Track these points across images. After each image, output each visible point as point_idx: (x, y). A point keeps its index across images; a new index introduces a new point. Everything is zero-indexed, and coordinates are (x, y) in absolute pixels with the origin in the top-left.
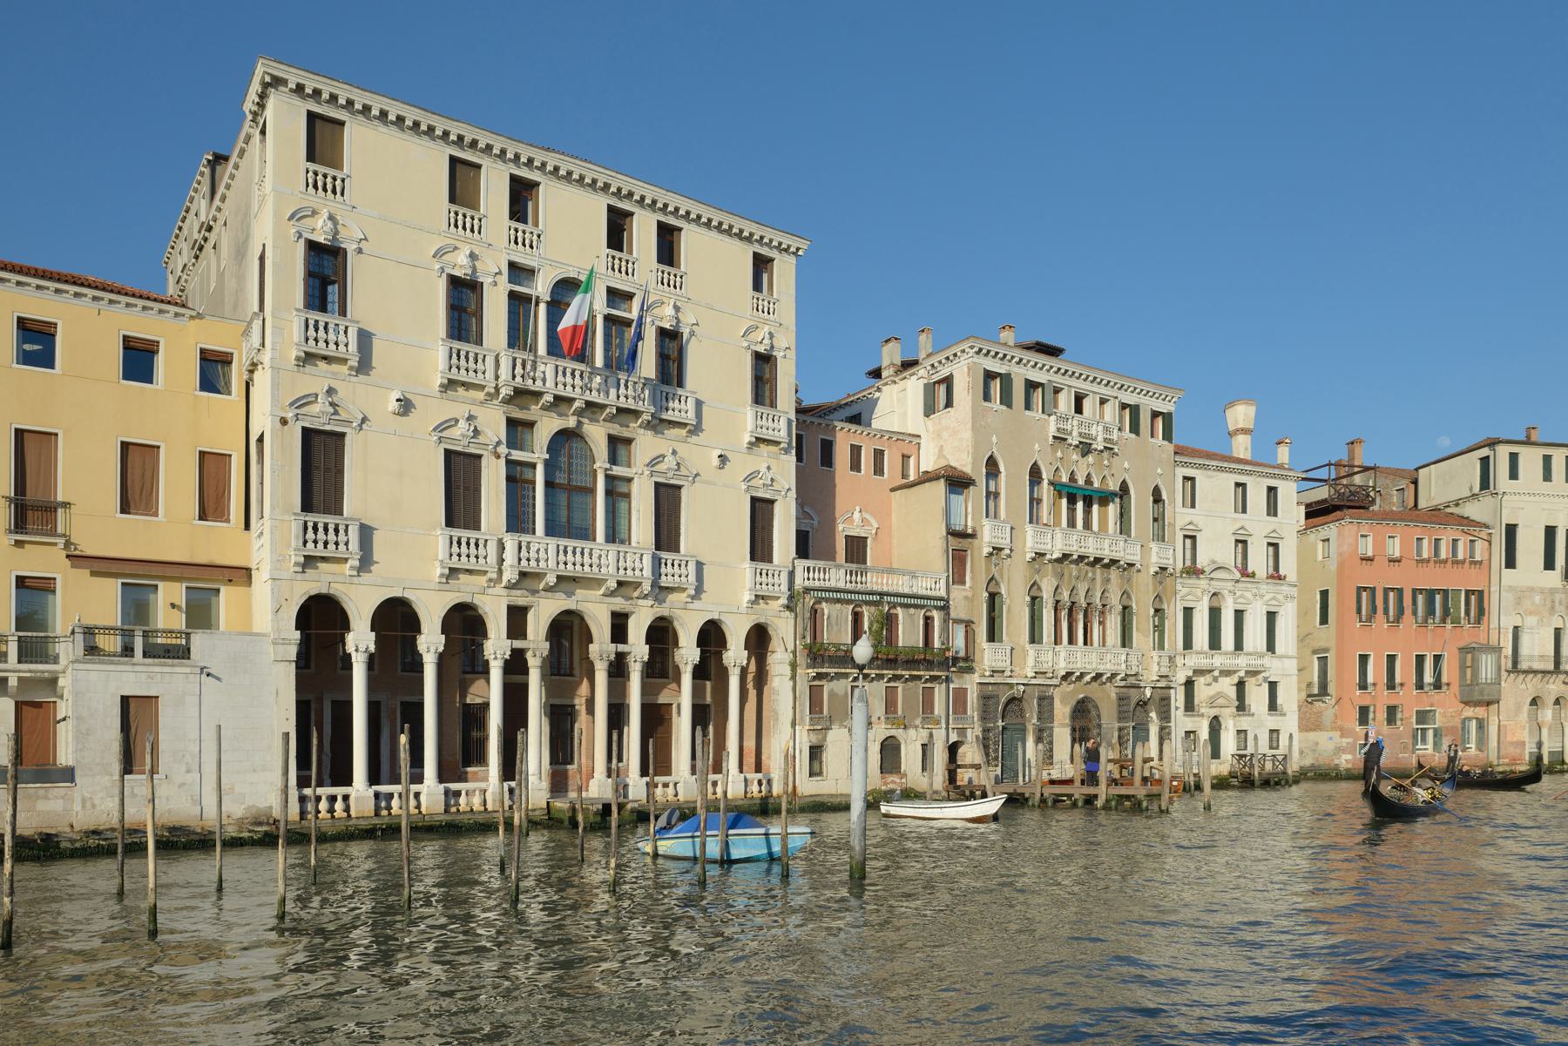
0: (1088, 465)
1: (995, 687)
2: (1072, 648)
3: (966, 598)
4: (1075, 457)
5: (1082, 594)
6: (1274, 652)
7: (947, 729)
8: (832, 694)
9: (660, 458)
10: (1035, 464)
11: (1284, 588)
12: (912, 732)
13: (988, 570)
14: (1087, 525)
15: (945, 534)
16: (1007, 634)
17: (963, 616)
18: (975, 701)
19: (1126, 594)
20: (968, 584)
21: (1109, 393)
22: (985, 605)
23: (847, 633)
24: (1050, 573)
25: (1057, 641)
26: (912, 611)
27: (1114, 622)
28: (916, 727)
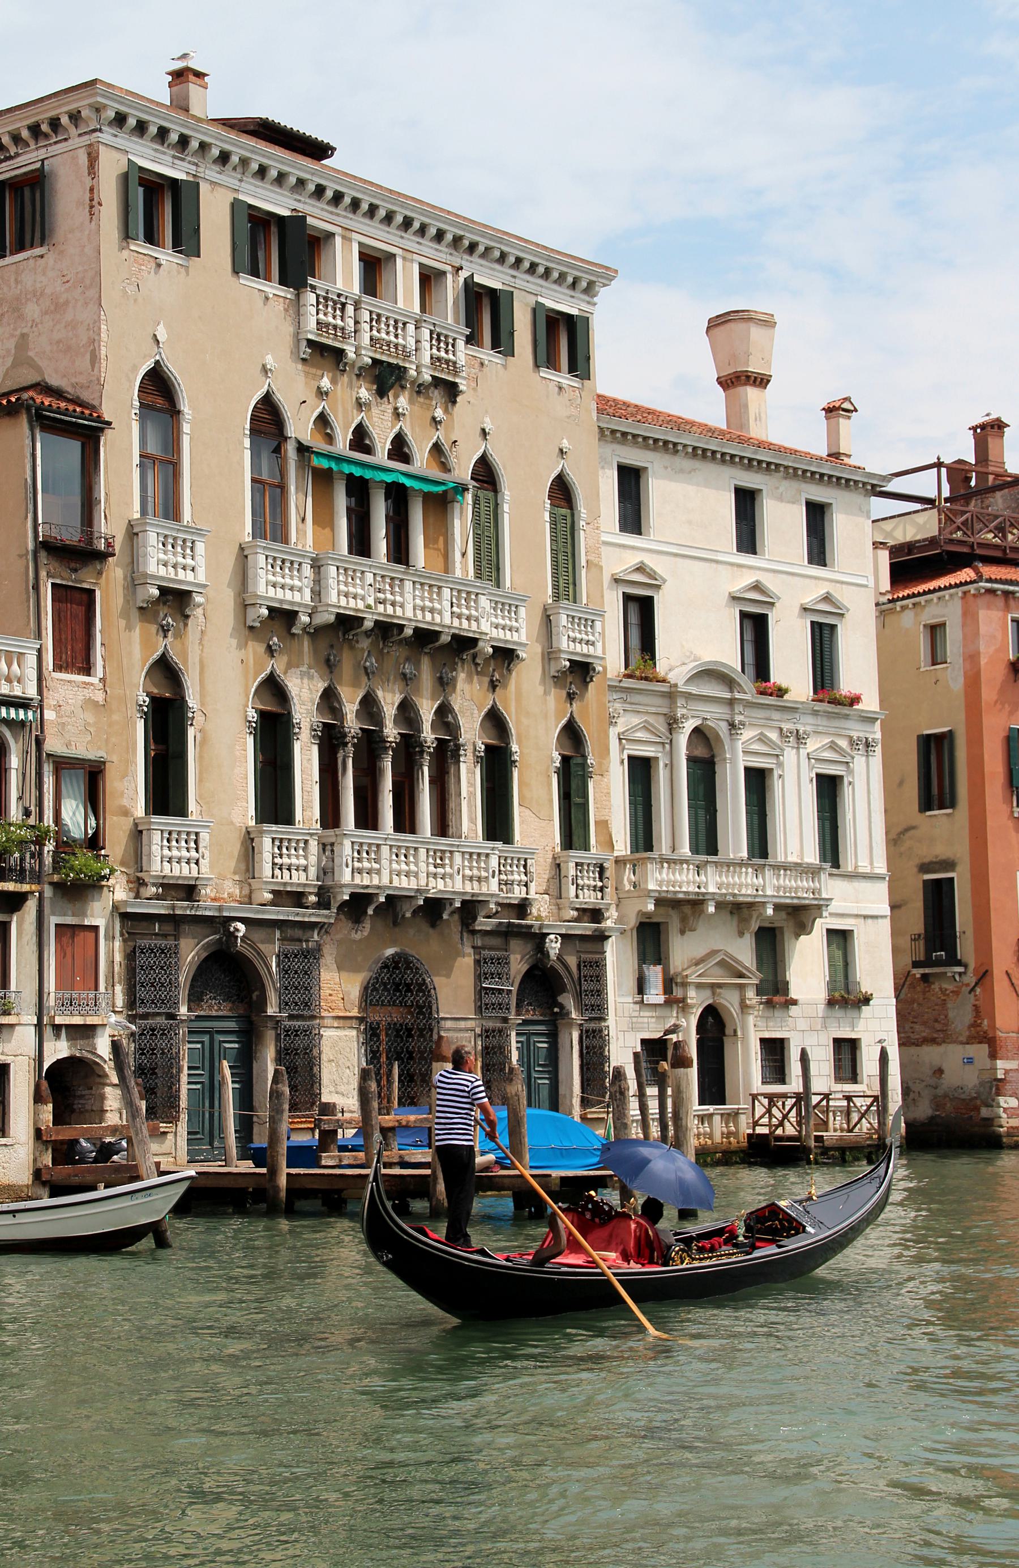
6: (836, 864)
7: (39, 1026)
11: (849, 724)
13: (147, 644)
14: (400, 553)
15: (31, 546)
17: (83, 749)
19: (495, 720)
20: (100, 673)
21: (443, 257)
22: (140, 725)
25: (330, 817)
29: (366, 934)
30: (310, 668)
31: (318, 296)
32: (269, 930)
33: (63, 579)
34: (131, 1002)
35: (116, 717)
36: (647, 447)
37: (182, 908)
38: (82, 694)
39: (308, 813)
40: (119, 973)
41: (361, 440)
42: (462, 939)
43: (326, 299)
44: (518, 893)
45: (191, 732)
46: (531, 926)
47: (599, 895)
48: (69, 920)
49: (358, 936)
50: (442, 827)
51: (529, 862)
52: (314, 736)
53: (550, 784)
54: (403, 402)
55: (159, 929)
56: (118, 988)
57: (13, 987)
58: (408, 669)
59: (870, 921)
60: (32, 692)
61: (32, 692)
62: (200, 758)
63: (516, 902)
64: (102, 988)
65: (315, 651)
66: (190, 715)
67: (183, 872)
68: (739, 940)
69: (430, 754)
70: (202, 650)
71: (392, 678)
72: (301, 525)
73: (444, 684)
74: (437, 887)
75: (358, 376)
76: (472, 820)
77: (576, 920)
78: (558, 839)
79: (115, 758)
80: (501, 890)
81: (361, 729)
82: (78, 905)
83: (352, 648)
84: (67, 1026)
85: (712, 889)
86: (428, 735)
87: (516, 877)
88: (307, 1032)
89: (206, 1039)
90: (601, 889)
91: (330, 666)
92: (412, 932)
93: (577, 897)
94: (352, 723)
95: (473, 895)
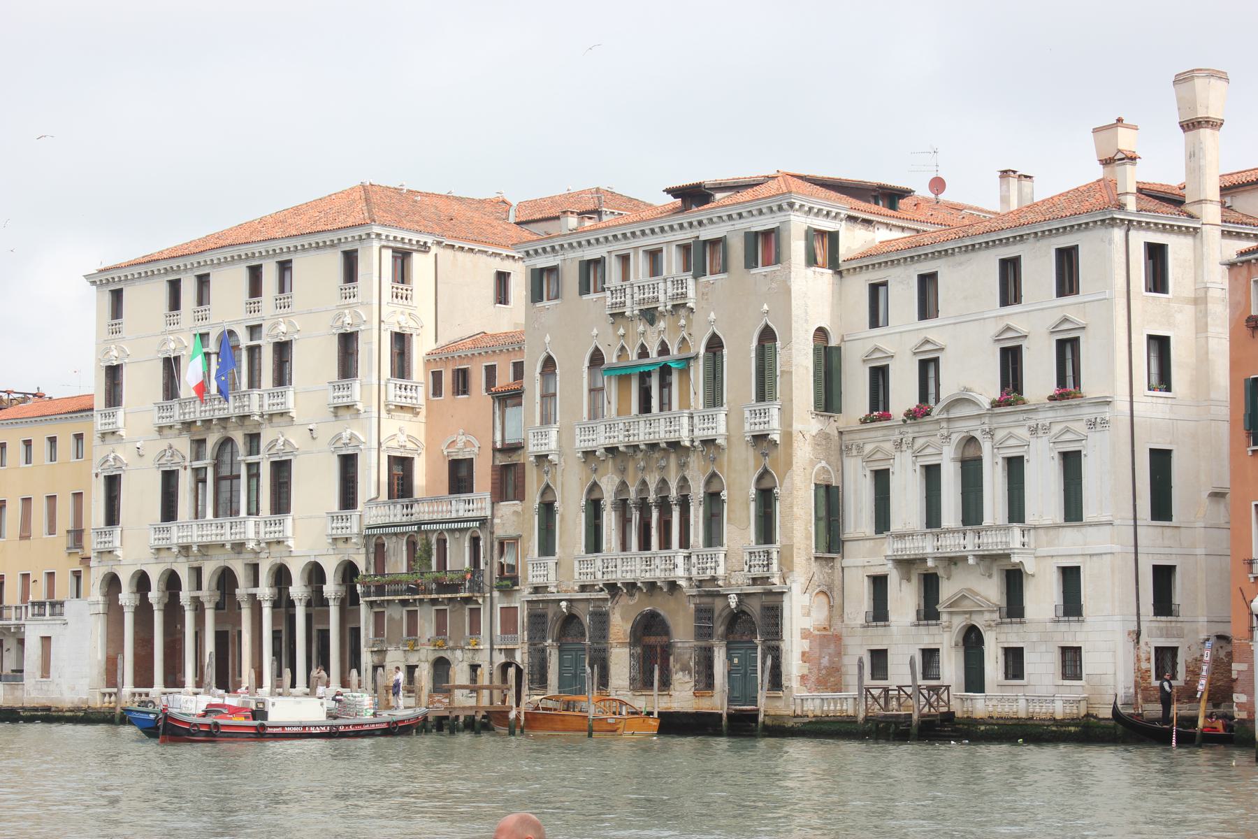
1: (545, 605)
2: (647, 554)
3: (516, 512)
4: (641, 328)
5: (652, 487)
7: (492, 649)
8: (391, 619)
9: (273, 443)
10: (597, 350)
12: (458, 653)
13: (539, 481)
16: (560, 545)
18: (525, 620)
21: (689, 236)
22: (536, 517)
23: (402, 563)
26: (457, 535)
27: (697, 515)
28: (462, 649)
31: (612, 291)
34: (530, 638)
35: (526, 516)
36: (933, 258)
37: (540, 597)
38: (512, 510)
41: (644, 353)
43: (616, 290)
44: (709, 573)
45: (557, 516)
46: (718, 591)
48: (505, 605)
50: (685, 543)
53: (748, 508)
54: (662, 324)
56: (526, 633)
58: (663, 463)
59: (1095, 558)
61: (488, 513)
62: (561, 528)
64: (519, 633)
65: (615, 465)
68: (989, 580)
69: (676, 504)
73: (683, 466)
74: (648, 576)
78: (753, 537)
79: (525, 535)
80: (698, 573)
81: (641, 498)
83: (633, 459)
85: (929, 550)
86: (674, 493)
87: (708, 565)
88: (604, 650)
89: (574, 653)
90: (768, 565)
91: (623, 471)
93: (749, 571)
94: (632, 495)
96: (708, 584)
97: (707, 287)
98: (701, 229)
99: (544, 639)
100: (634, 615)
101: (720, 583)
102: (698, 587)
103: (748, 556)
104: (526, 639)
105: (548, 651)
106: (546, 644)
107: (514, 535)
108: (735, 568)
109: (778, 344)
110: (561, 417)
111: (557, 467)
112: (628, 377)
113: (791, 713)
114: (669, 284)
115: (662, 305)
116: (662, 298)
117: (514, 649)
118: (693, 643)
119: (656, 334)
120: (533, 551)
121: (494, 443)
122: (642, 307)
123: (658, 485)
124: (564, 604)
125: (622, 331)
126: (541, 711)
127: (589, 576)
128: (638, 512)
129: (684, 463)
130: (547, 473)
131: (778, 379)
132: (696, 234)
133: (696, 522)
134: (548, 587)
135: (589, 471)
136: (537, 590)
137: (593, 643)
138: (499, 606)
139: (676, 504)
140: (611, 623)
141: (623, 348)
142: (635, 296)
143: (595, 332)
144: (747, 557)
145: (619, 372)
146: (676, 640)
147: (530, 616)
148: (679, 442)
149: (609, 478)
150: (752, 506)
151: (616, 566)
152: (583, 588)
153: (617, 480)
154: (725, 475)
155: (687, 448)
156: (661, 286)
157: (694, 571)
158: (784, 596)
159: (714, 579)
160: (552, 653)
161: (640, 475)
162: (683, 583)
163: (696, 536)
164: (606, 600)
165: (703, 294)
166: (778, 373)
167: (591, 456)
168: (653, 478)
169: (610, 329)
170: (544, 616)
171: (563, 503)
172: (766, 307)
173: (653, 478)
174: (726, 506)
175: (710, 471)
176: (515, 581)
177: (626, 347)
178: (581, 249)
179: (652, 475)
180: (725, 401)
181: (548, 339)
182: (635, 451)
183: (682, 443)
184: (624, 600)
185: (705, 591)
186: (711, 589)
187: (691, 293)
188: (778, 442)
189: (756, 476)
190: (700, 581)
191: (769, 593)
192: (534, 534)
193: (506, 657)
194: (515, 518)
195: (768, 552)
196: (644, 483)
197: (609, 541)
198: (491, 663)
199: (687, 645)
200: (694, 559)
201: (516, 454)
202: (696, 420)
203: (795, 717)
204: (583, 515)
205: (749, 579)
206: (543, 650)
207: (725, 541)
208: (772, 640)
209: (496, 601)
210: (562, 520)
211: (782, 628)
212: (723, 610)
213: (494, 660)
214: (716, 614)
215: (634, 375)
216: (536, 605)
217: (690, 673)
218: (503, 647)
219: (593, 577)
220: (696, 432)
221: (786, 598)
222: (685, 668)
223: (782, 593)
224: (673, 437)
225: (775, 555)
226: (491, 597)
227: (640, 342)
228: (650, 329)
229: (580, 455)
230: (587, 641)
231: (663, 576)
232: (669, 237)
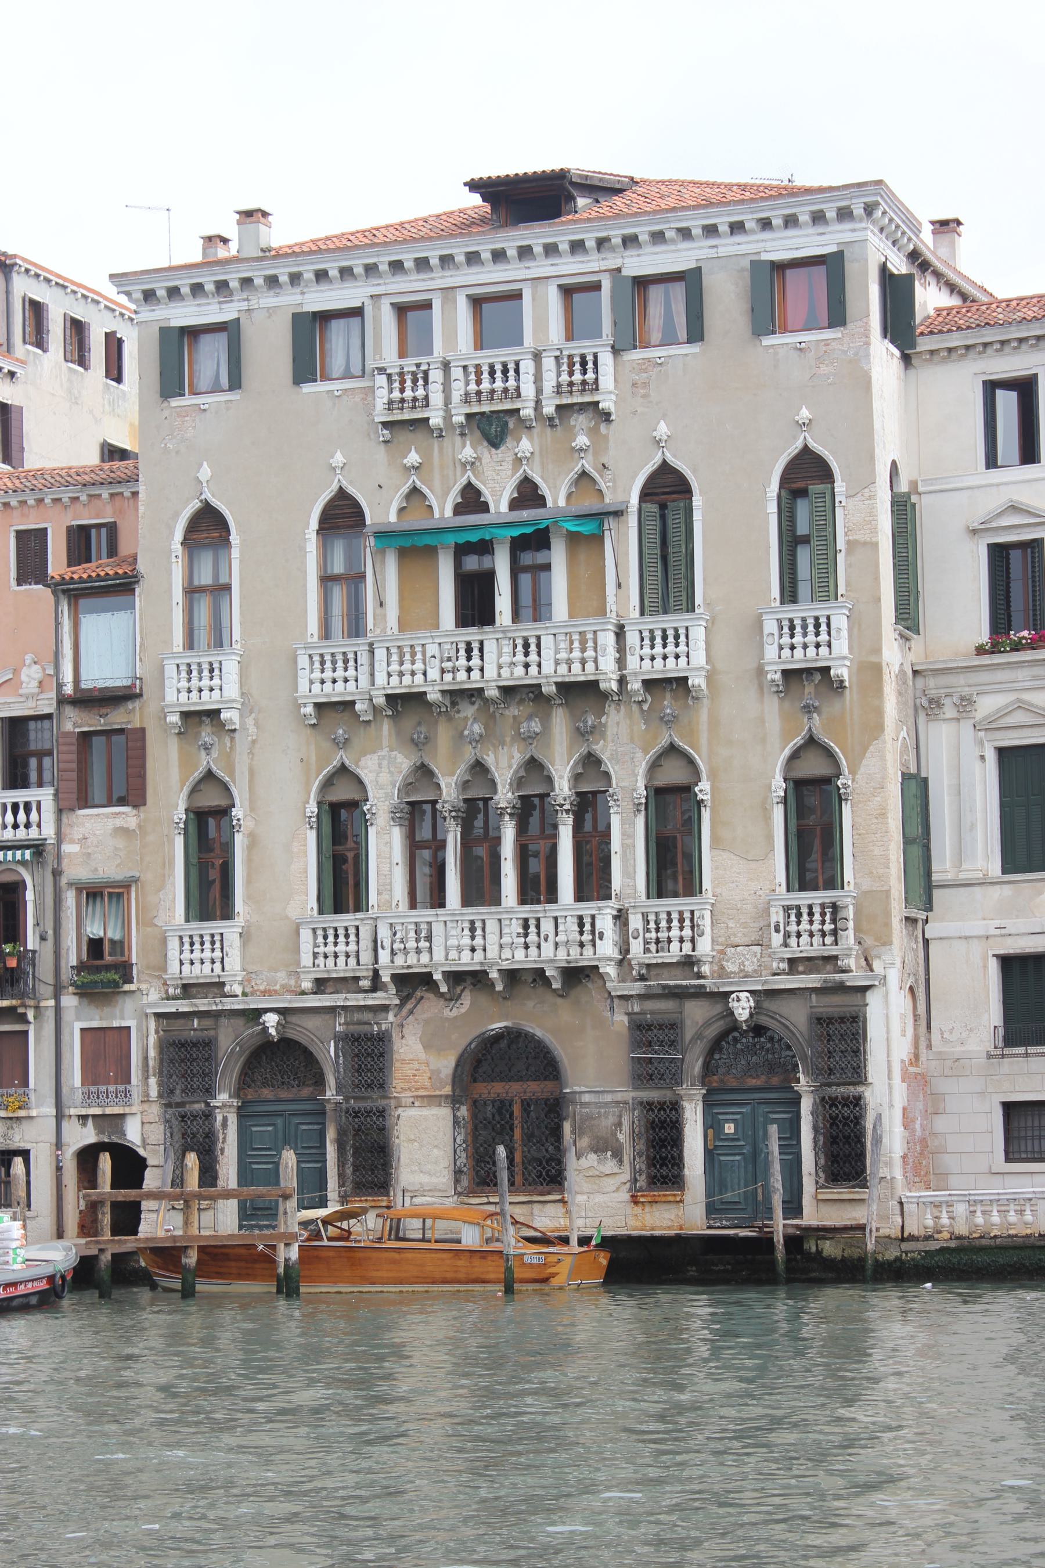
0: (518, 461)
1: (208, 1022)
3: (123, 832)
4: (468, 452)
7: (59, 1117)
13: (186, 763)
16: (248, 898)
18: (152, 1053)
21: (594, 266)
22: (179, 842)
24: (385, 742)
29: (463, 1010)
30: (391, 750)
31: (389, 376)
32: (327, 1017)
33: (90, 726)
34: (167, 1091)
37: (203, 1004)
38: (111, 824)
39: (386, 896)
40: (154, 1067)
42: (612, 1009)
44: (675, 952)
46: (703, 986)
47: (829, 940)
48: (95, 1024)
49: (447, 1013)
51: (697, 914)
52: (393, 819)
53: (768, 818)
54: (525, 445)
55: (199, 1024)
56: (153, 1081)
57: (32, 1085)
58: (536, 726)
60: (49, 831)
61: (49, 831)
62: (249, 861)
63: (674, 960)
64: (134, 1080)
65: (399, 733)
66: (235, 822)
67: (201, 972)
69: (567, 811)
70: (252, 759)
71: (508, 739)
72: (379, 610)
75: (462, 435)
76: (629, 874)
77: (782, 973)
79: (148, 877)
80: (647, 950)
81: (466, 801)
82: (106, 1010)
83: (450, 719)
84: (94, 1116)
88: (382, 1113)
90: (835, 932)
92: (530, 1004)
93: (786, 945)
95: (569, 962)
96: (665, 972)
97: (645, 371)
98: (628, 253)
99: (209, 1092)
100: (462, 1039)
101: (706, 969)
102: (642, 978)
103: (781, 913)
104: (154, 1092)
105: (219, 1118)
106: (214, 1103)
107: (119, 877)
108: (737, 940)
109: (840, 486)
110: (243, 632)
111: (237, 735)
112: (431, 551)
113: (895, 1232)
114: (548, 363)
115: (532, 404)
116: (528, 390)
117: (122, 1116)
118: (629, 1095)
119: (508, 466)
120: (172, 909)
121: (60, 686)
122: (476, 409)
123: (516, 772)
124: (271, 1020)
125: (413, 458)
126: (326, 1243)
127: (341, 960)
128: (459, 829)
129: (593, 727)
130: (207, 748)
131: (841, 558)
132: (613, 263)
133: (628, 848)
134: (223, 984)
135: (327, 745)
136: (188, 990)
137: (347, 1099)
138: (78, 1026)
139: (567, 811)
140: (396, 1056)
141: (415, 491)
142: (455, 385)
143: (339, 459)
144: (777, 916)
145: (407, 543)
146: (577, 1089)
147: (164, 1046)
148: (596, 683)
149: (381, 758)
150: (778, 814)
151: (429, 938)
152: (321, 985)
153: (404, 763)
154: (704, 750)
155: (605, 696)
156: (527, 366)
157: (636, 947)
158: (869, 994)
159: (689, 963)
160: (229, 1123)
161: (469, 754)
162: (610, 970)
163: (629, 874)
164: (385, 1008)
165: (634, 385)
166: (841, 544)
167: (331, 715)
168: (504, 762)
169: (381, 454)
170: (209, 1044)
171: (252, 809)
172: (805, 414)
173: (504, 762)
174: (706, 815)
175: (663, 742)
176: (125, 971)
177: (425, 490)
178: (298, 290)
179: (503, 753)
180: (698, 599)
181: (205, 473)
182: (454, 704)
183: (603, 686)
184: (430, 1008)
185: (665, 987)
186: (684, 983)
187: (607, 381)
188: (847, 684)
189: (787, 752)
190: (648, 966)
191: (841, 988)
192: (172, 874)
193: (100, 1130)
194: (121, 843)
195: (835, 907)
196: (479, 768)
197: (386, 888)
198: (59, 1145)
199: (608, 1098)
200: (635, 922)
201: (122, 710)
202: (632, 638)
203: (903, 1239)
204: (312, 836)
205: (782, 960)
206: (208, 1115)
207: (706, 884)
208: (838, 1085)
209: (68, 1016)
210: (253, 841)
211: (865, 1060)
212: (707, 1024)
213: (66, 1137)
214: (689, 1034)
215: (445, 547)
216: (181, 1021)
217: (614, 1156)
218: (97, 1111)
219: (352, 961)
220: (632, 663)
221: (871, 997)
222: (604, 1146)
223: (865, 989)
224: (577, 674)
225: (850, 913)
226: (58, 1009)
227: (463, 481)
228: (487, 454)
229: (309, 710)
230: (331, 1093)
231: (562, 954)
232: (541, 267)
